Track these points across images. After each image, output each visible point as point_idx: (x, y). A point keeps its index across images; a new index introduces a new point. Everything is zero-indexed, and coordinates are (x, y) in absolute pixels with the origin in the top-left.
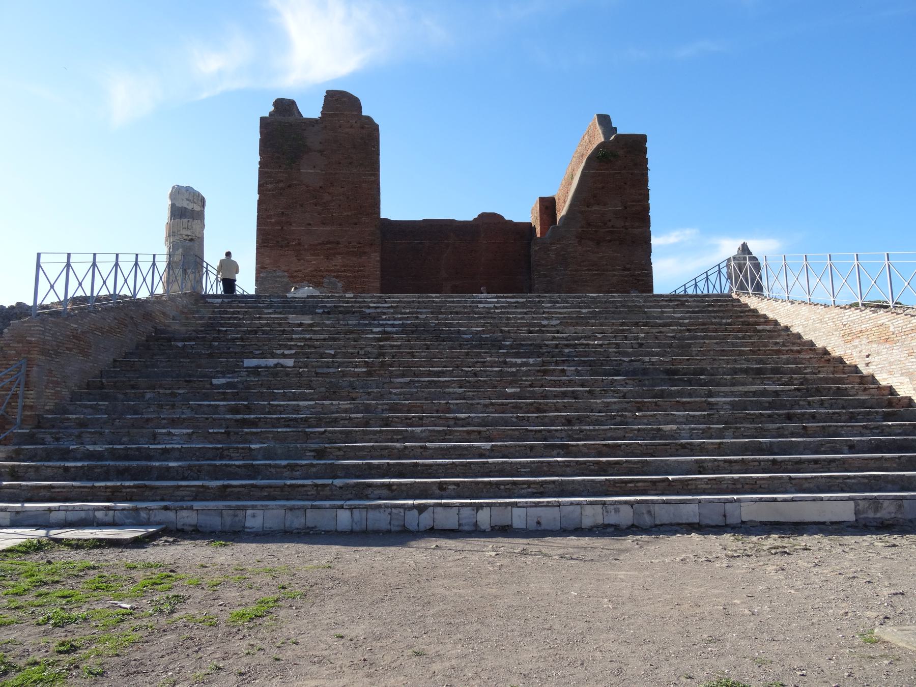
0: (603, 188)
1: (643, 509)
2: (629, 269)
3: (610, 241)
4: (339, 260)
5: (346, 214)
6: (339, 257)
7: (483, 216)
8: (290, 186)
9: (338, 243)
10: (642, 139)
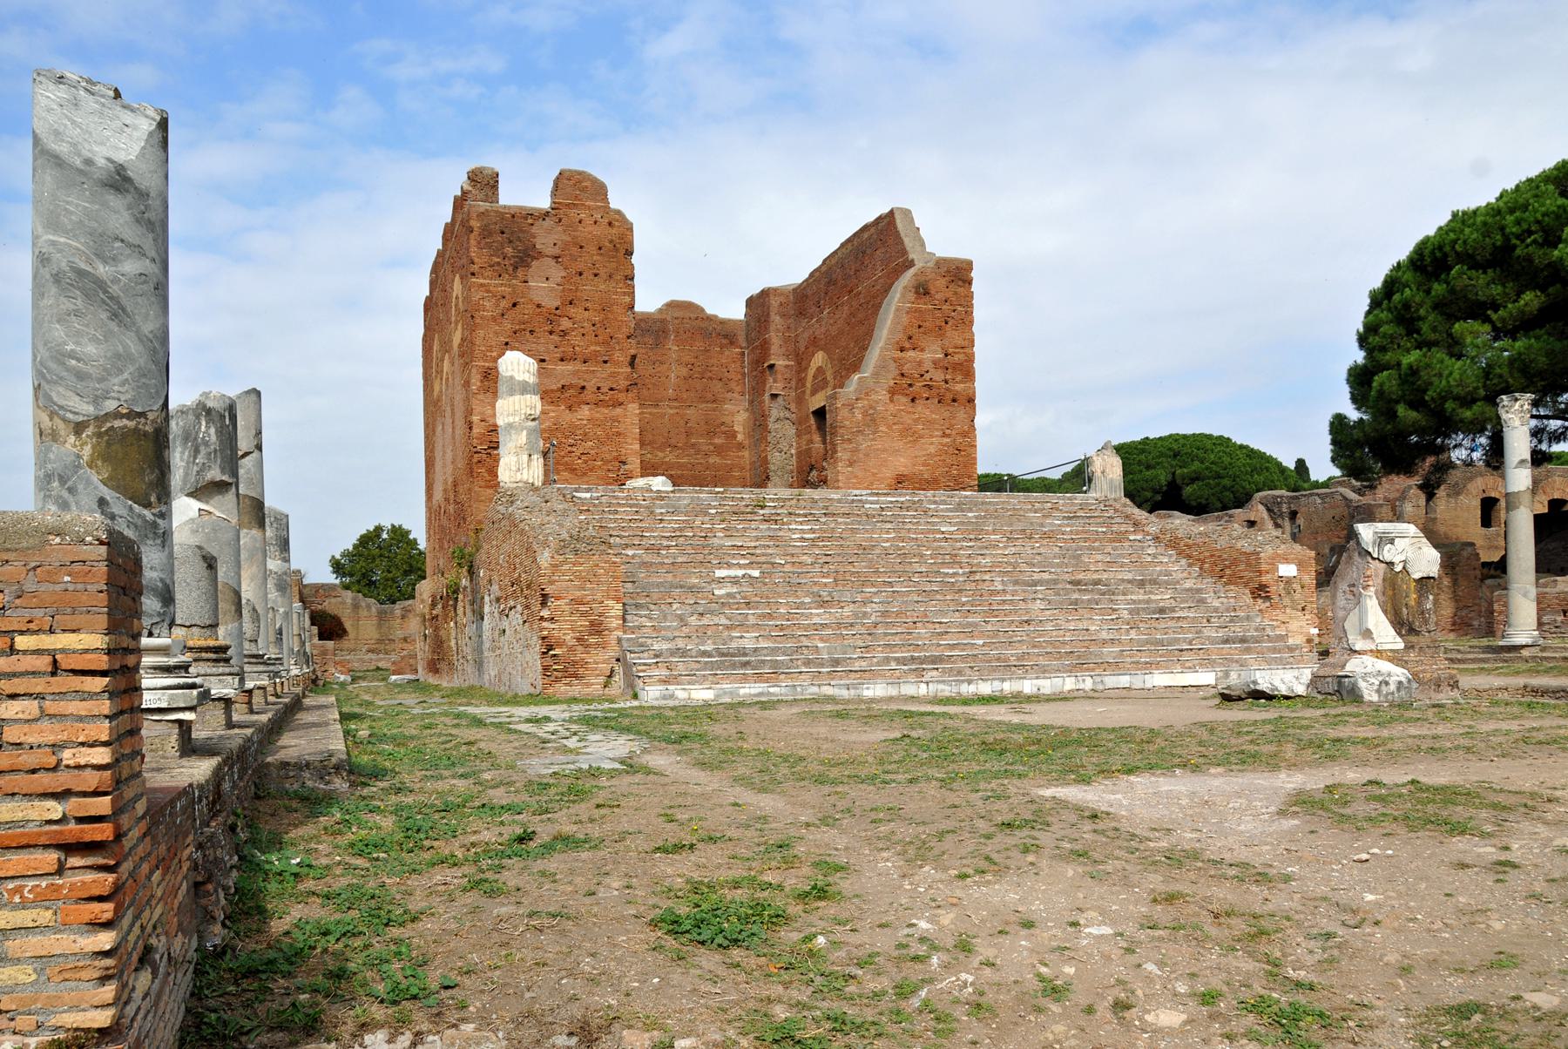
1: (1098, 679)
2: (948, 436)
4: (585, 411)
6: (586, 407)
7: (672, 305)
8: (514, 305)
10: (969, 265)
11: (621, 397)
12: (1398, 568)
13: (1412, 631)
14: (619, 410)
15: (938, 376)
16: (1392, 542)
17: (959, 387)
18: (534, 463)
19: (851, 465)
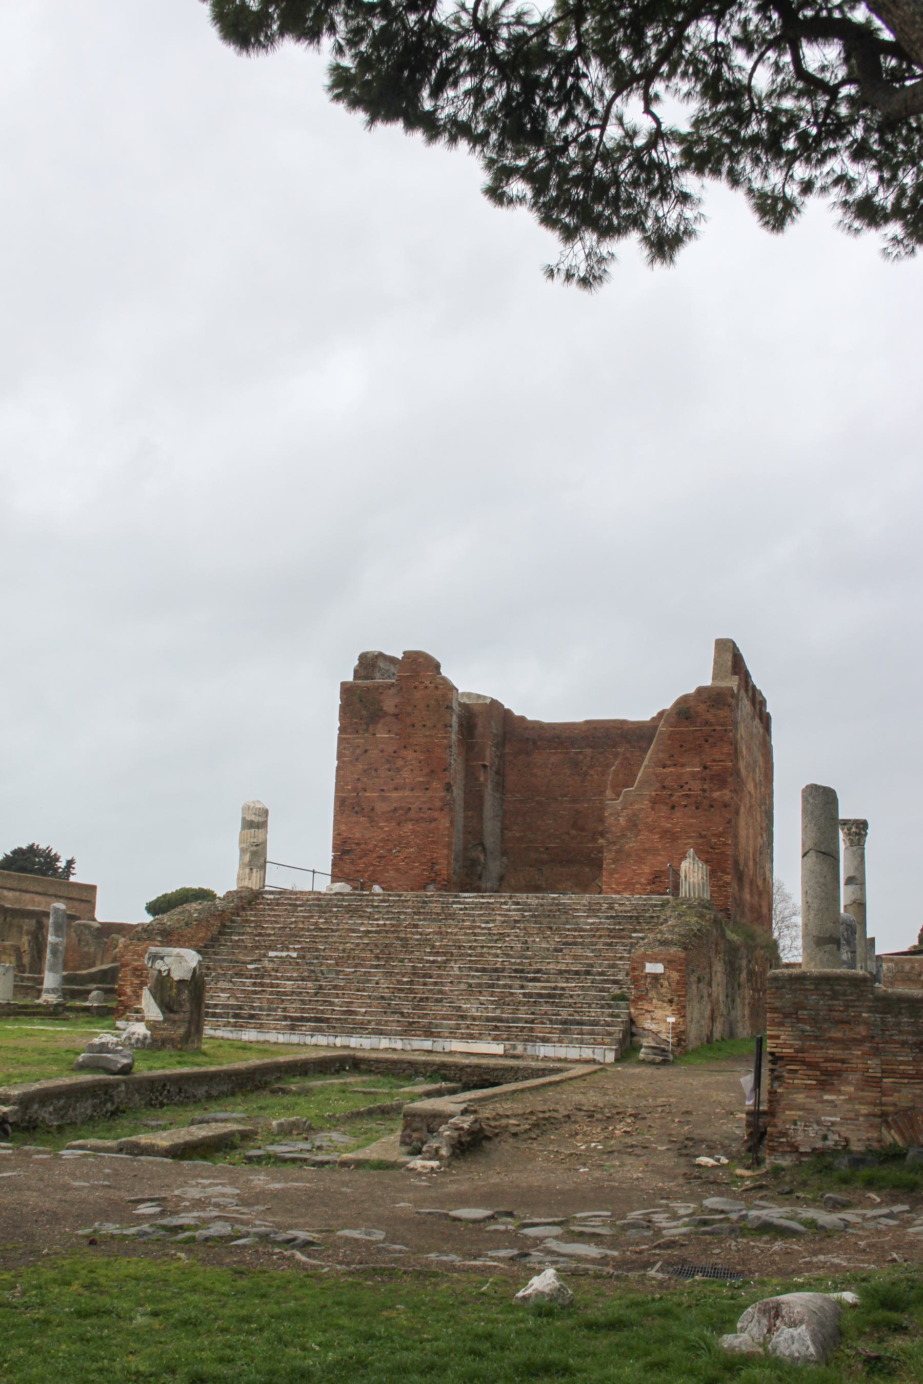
0: (681, 746)
3: (685, 806)
5: (418, 779)
8: (366, 751)
9: (410, 809)
11: (436, 814)
12: (165, 974)
13: (171, 1011)
14: (434, 825)
15: (696, 785)
16: (162, 958)
17: (716, 795)
18: (254, 874)
19: (614, 863)
